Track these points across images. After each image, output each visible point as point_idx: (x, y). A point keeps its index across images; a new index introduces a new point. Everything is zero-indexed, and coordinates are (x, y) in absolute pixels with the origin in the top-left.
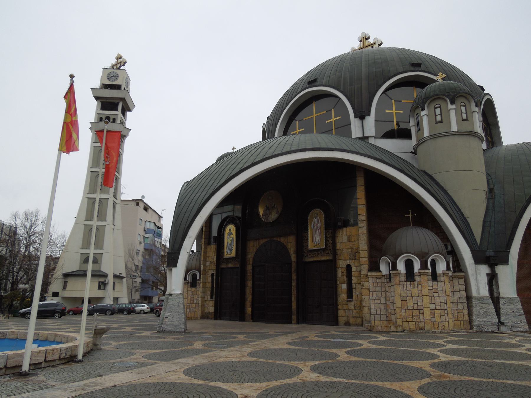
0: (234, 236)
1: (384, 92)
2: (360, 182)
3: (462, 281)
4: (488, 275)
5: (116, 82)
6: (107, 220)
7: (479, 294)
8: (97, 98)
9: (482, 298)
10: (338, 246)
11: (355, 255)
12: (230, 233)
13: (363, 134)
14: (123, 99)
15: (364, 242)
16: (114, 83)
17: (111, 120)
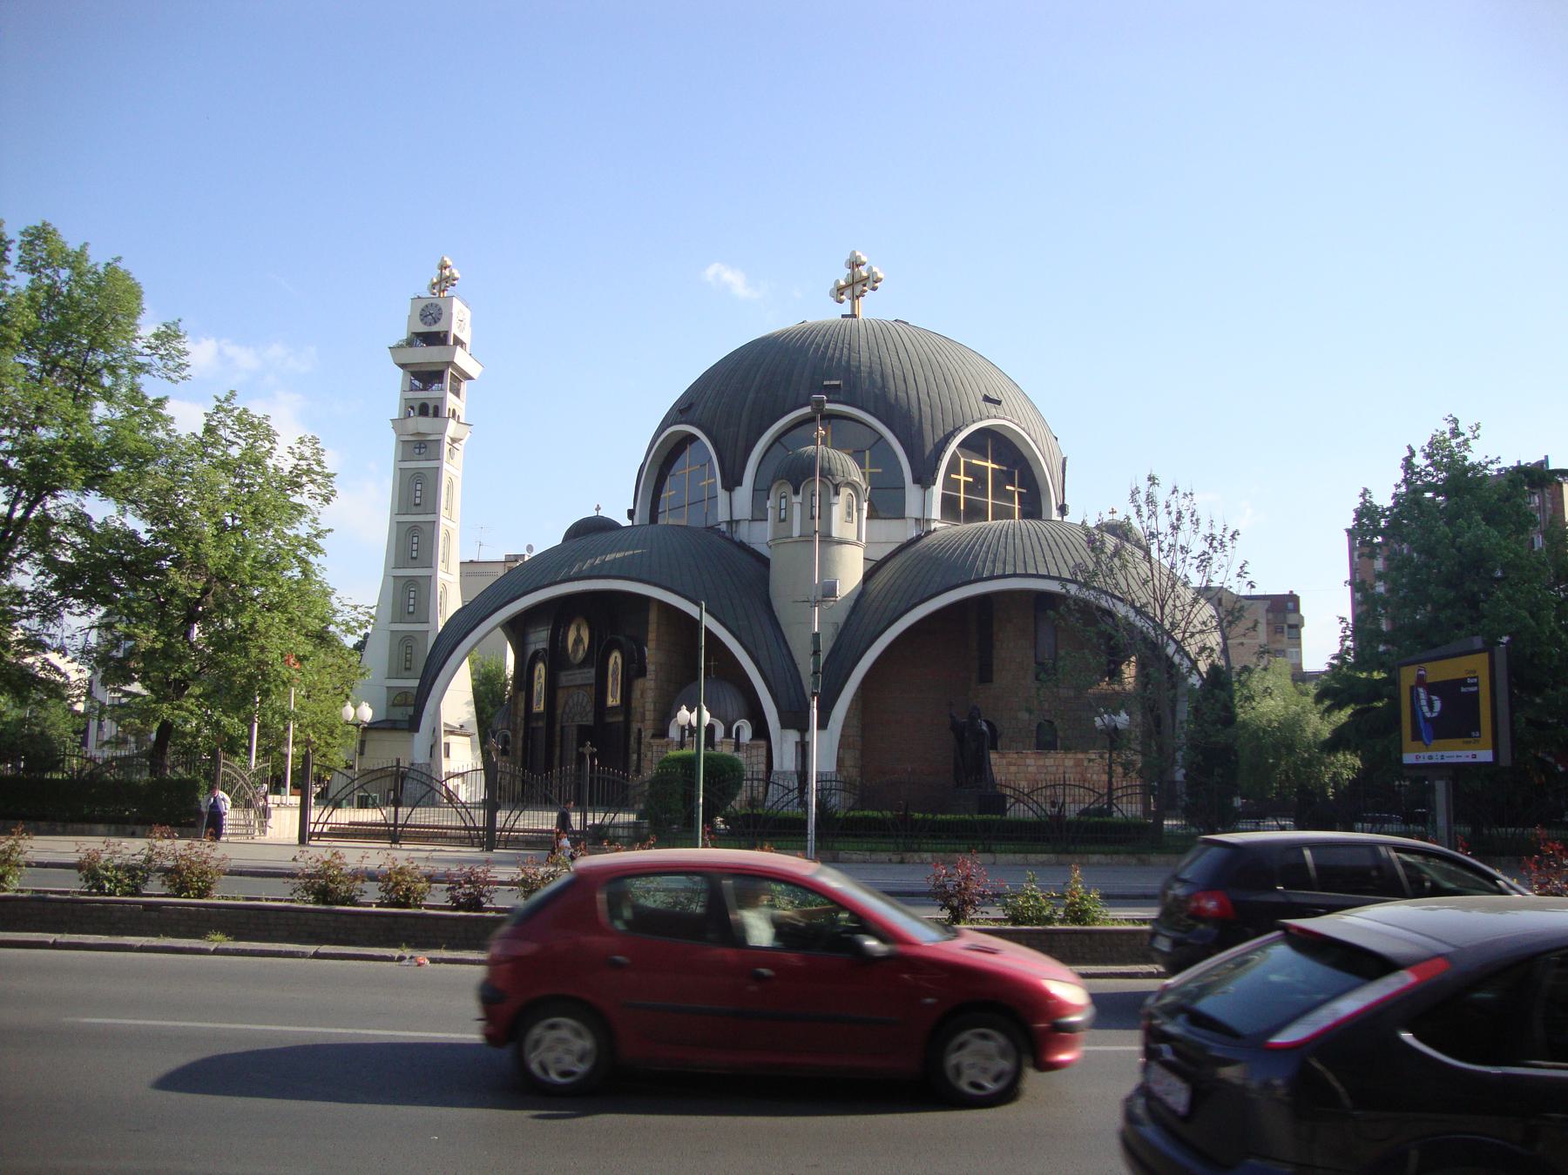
0: (542, 680)
1: (778, 439)
2: (653, 616)
3: (763, 752)
4: (797, 743)
5: (437, 325)
6: (430, 620)
7: (782, 768)
8: (402, 366)
9: (784, 773)
10: (634, 704)
11: (643, 720)
12: (540, 677)
13: (731, 517)
14: (451, 363)
15: (650, 700)
16: (434, 328)
17: (431, 411)
